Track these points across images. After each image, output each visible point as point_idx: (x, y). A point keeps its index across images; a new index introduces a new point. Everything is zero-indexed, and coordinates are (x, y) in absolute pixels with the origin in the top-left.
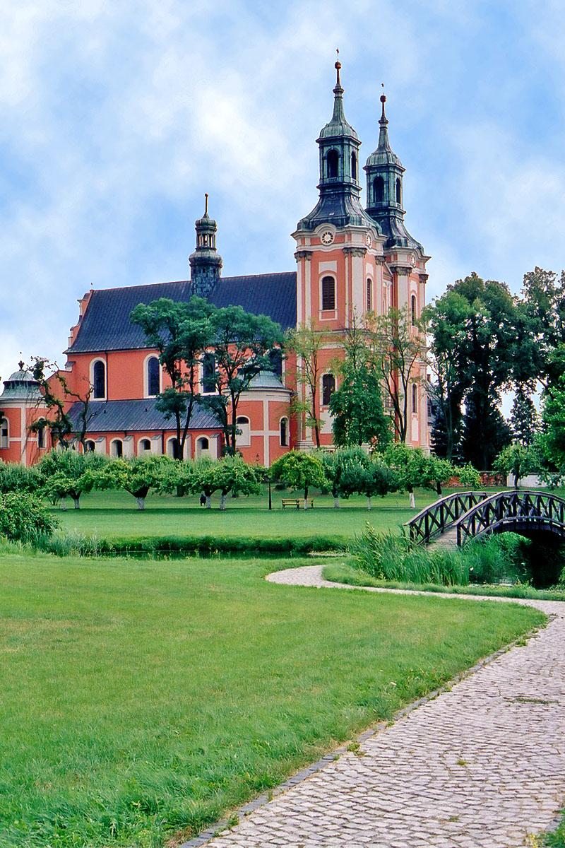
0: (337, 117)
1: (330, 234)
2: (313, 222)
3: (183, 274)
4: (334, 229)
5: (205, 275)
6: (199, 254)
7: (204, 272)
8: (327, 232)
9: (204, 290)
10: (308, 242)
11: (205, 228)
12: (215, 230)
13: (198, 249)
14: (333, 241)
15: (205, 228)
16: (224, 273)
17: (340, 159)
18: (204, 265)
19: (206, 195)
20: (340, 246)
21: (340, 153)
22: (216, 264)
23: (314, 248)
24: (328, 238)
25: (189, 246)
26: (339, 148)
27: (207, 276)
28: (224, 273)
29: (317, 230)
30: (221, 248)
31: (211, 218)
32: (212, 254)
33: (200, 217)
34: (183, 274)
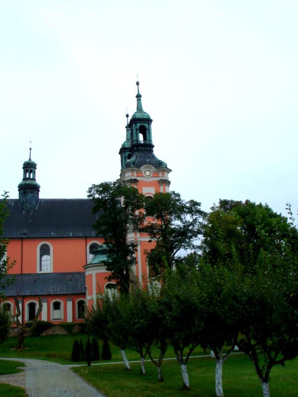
0: (139, 108)
1: (149, 171)
2: (137, 163)
3: (15, 195)
4: (154, 168)
5: (32, 195)
6: (24, 182)
7: (32, 193)
8: (149, 170)
9: (32, 204)
10: (135, 174)
11: (29, 167)
12: (36, 168)
13: (25, 179)
14: (151, 175)
15: (29, 167)
16: (43, 195)
17: (147, 131)
18: (29, 188)
19: (30, 149)
20: (158, 179)
21: (147, 128)
22: (36, 188)
23: (138, 179)
24: (148, 173)
25: (18, 177)
26: (146, 125)
27: (34, 196)
28: (43, 195)
29: (142, 168)
30: (40, 178)
31: (34, 160)
32: (33, 182)
33: (27, 160)
34: (15, 195)
